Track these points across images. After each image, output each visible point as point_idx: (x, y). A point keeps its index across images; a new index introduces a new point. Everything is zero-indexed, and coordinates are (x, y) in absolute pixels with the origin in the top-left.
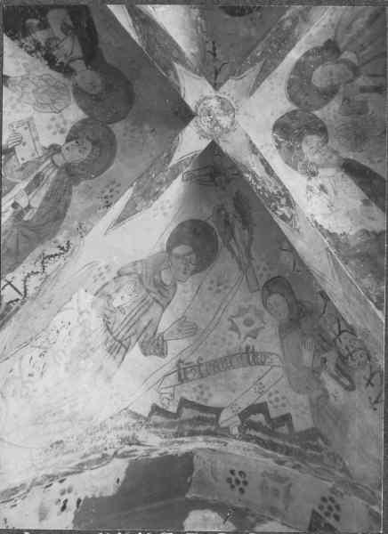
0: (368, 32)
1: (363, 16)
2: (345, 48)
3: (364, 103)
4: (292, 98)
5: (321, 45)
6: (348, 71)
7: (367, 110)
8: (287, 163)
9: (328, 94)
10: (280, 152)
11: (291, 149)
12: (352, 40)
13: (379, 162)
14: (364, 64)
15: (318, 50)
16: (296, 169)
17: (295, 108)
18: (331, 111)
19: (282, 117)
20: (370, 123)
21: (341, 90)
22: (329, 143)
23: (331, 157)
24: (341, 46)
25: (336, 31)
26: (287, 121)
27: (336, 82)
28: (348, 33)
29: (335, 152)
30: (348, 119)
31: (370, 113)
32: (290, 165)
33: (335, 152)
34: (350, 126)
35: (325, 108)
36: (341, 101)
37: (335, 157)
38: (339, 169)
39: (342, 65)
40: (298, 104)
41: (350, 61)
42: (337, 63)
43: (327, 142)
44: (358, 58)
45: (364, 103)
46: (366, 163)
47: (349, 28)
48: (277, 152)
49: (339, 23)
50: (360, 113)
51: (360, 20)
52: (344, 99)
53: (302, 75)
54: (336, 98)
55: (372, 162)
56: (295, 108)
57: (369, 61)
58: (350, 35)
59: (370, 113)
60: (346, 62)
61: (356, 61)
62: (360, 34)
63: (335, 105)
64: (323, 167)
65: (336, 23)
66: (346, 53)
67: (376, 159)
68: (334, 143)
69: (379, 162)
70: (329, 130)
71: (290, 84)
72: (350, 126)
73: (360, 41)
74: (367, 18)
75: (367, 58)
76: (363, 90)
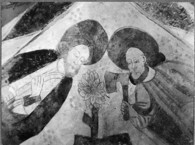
0: (170, 86)
1: (184, 81)
2: (157, 70)
3: (115, 89)
4: (118, 34)
5: (162, 50)
6: (139, 75)
7: (109, 93)
8: (67, 32)
9: (121, 62)
10: (75, 26)
11: (77, 36)
12: (164, 75)
13: (71, 105)
14: (144, 86)
15: (156, 48)
16: (61, 41)
17: (109, 38)
18: (107, 65)
19: (102, 28)
20: (100, 96)
21: (125, 72)
22: (85, 66)
23: (73, 68)
24: (160, 67)
25: (172, 61)
26: (100, 32)
27: (130, 66)
28: (170, 71)
29: (77, 72)
30: (103, 79)
31: (108, 95)
32: (65, 34)
33: (77, 72)
34: (98, 80)
35: (110, 61)
36: (116, 72)
37: (73, 71)
38: (64, 76)
39: (143, 69)
40: (112, 39)
41: (146, 76)
42: (145, 65)
43: (84, 64)
44: (147, 82)
45: (115, 89)
46: (69, 96)
47: (174, 71)
48: (75, 23)
49: (177, 63)
50: (107, 87)
51: (180, 78)
52: (117, 75)
53: (135, 39)
54: (118, 68)
55: (71, 100)
56: (109, 38)
57: (147, 90)
58: (168, 73)
59: (108, 95)
60: (147, 70)
61: (147, 80)
62: (171, 80)
63: (114, 68)
64: (65, 62)
65: (178, 60)
66: (154, 71)
67: (73, 103)
68: (84, 69)
69: (71, 105)
70: (93, 65)
71: (127, 30)
72: (98, 80)
73: (163, 81)
74: (183, 84)
75: (150, 88)
76: (125, 88)
